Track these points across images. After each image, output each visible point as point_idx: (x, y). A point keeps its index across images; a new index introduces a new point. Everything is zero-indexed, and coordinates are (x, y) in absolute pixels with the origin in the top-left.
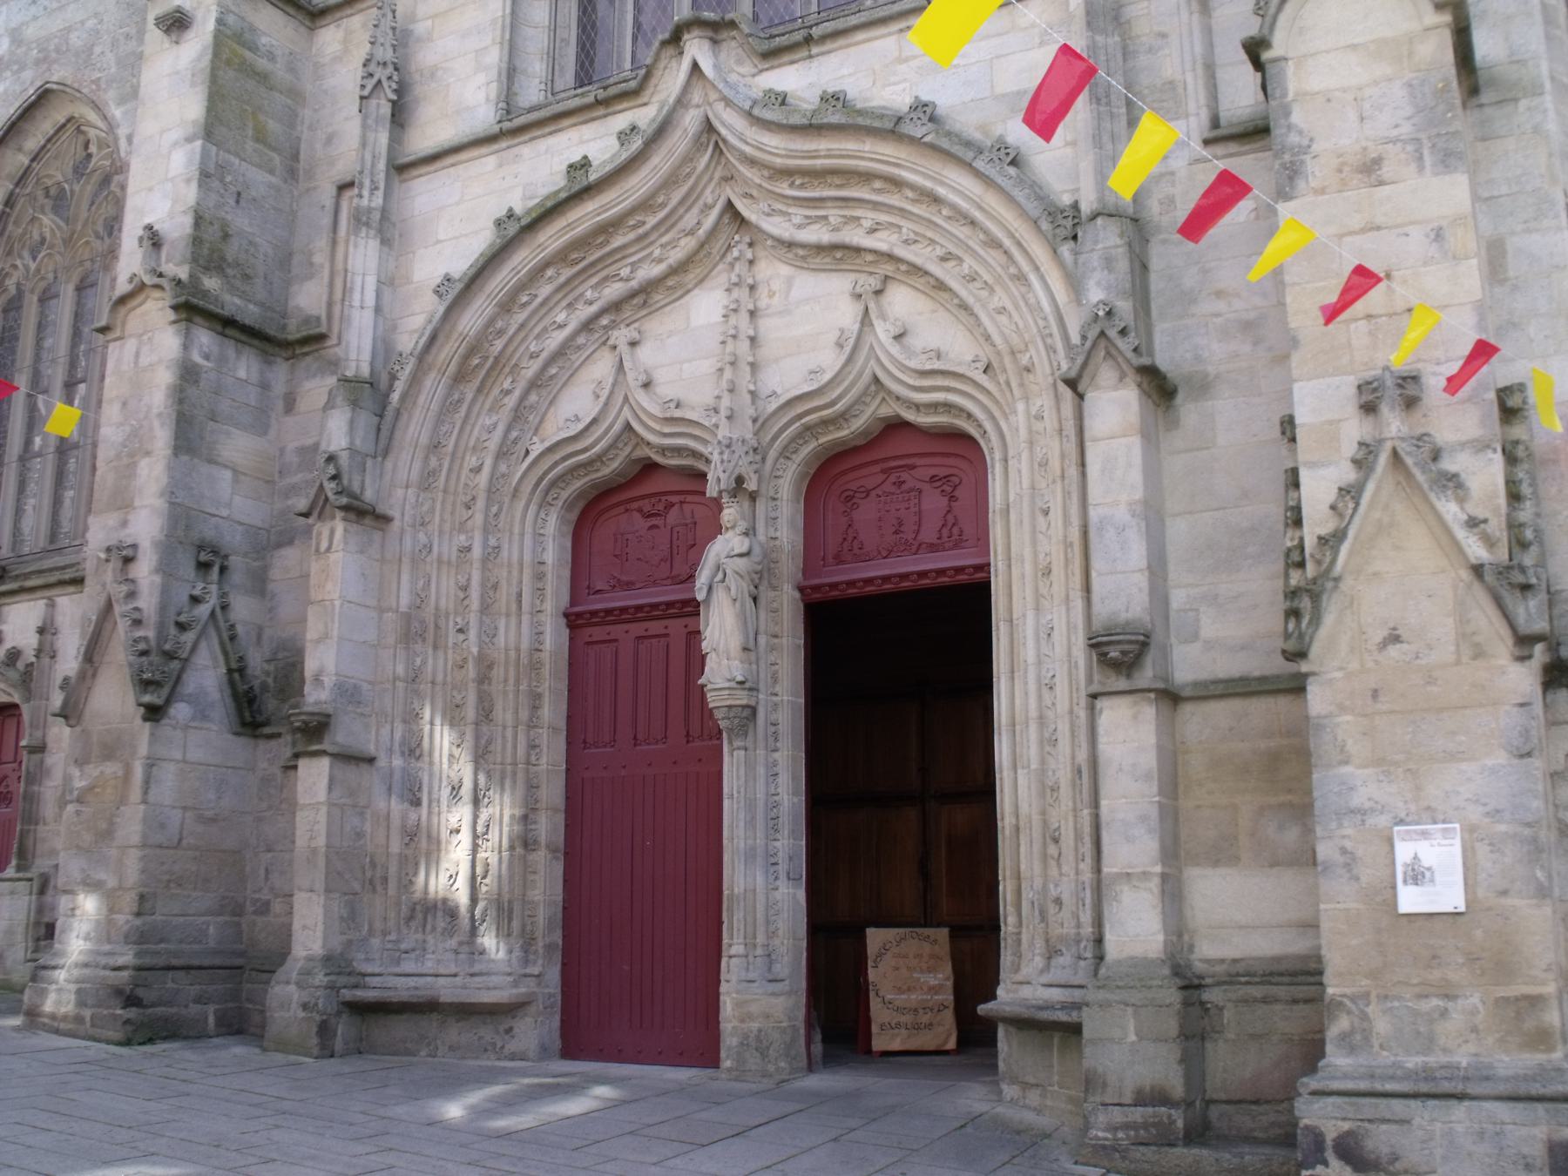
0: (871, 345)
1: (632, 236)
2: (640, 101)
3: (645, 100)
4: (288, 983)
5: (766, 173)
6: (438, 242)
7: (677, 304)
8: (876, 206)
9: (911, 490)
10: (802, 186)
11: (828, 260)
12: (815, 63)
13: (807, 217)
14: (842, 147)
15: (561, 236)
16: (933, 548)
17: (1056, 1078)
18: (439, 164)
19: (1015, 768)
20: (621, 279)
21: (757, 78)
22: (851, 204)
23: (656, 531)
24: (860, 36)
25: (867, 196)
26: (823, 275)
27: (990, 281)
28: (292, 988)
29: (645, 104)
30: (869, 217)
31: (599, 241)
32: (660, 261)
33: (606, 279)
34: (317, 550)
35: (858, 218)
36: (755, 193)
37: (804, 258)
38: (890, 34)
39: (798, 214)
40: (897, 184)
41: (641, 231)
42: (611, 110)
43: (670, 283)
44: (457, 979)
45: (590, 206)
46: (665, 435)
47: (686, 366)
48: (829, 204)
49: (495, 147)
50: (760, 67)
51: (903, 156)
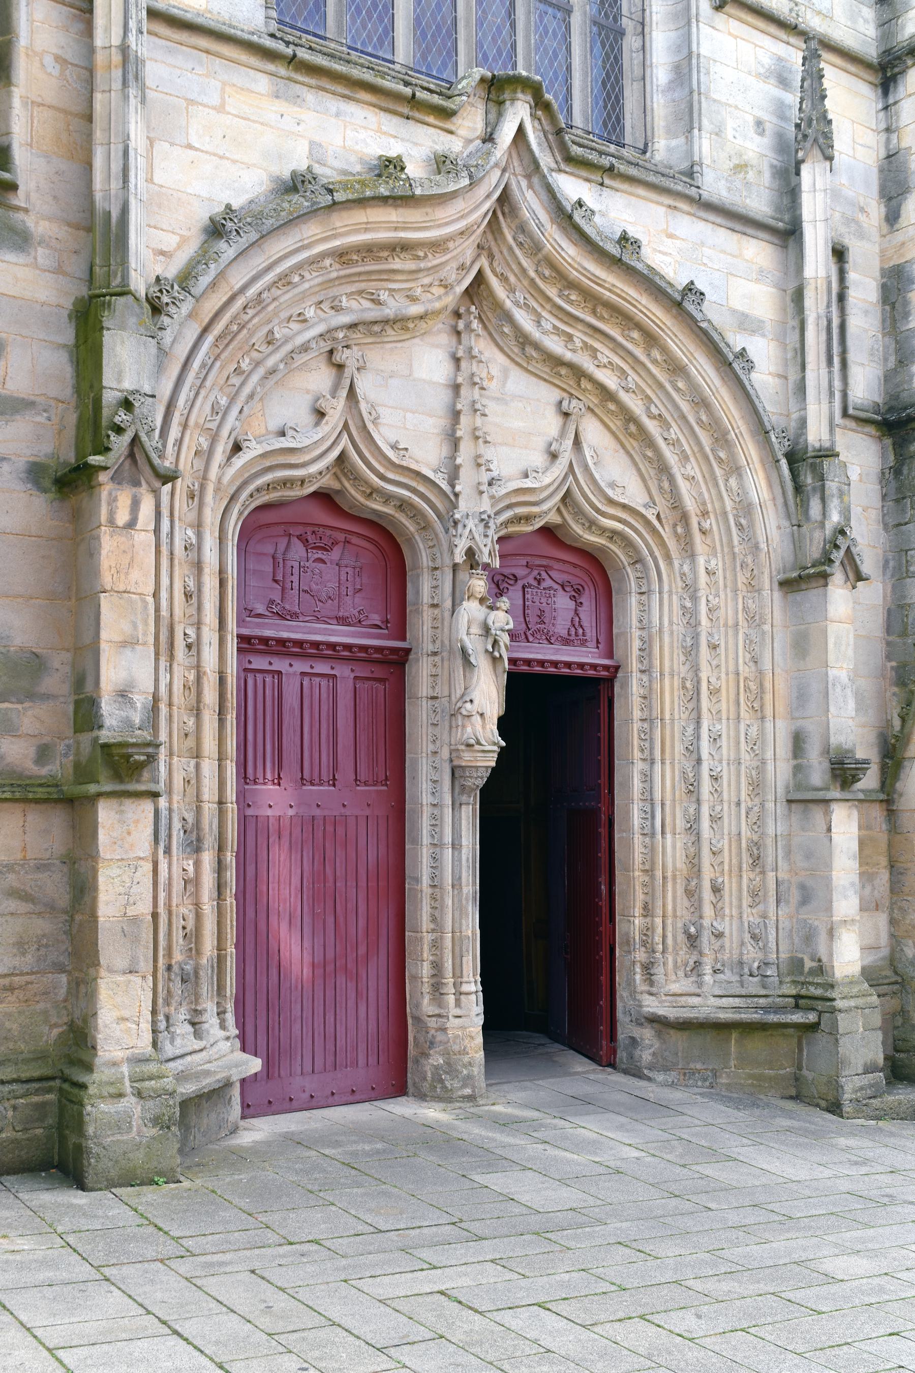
0: (571, 463)
1: (411, 265)
2: (448, 126)
3: (453, 128)
4: (121, 1095)
5: (547, 273)
6: (190, 147)
7: (399, 345)
8: (617, 347)
9: (550, 588)
10: (571, 302)
11: (547, 370)
12: (606, 192)
13: (555, 327)
14: (626, 289)
15: (357, 231)
16: (566, 642)
17: (732, 1063)
18: (184, 36)
19: (663, 833)
20: (373, 300)
21: (554, 174)
22: (597, 336)
23: (321, 565)
24: (641, 191)
25: (620, 339)
26: (534, 380)
27: (689, 452)
28: (130, 1103)
29: (451, 132)
30: (606, 354)
31: (381, 254)
32: (413, 299)
33: (360, 292)
34: (111, 522)
35: (595, 350)
36: (512, 279)
37: (529, 359)
38: (662, 204)
39: (549, 321)
40: (651, 339)
41: (422, 265)
42: (417, 115)
43: (411, 325)
44: (204, 1053)
45: (393, 215)
46: (382, 477)
47: (409, 415)
48: (580, 327)
49: (271, 67)
50: (563, 166)
51: (669, 323)
